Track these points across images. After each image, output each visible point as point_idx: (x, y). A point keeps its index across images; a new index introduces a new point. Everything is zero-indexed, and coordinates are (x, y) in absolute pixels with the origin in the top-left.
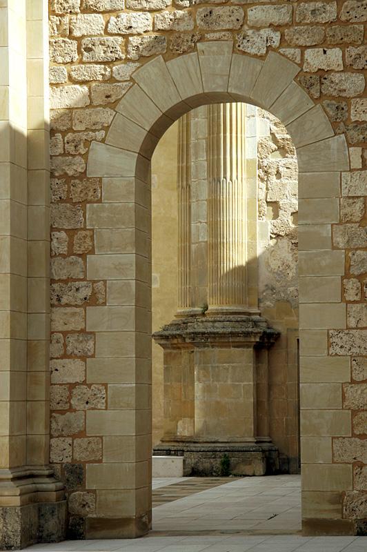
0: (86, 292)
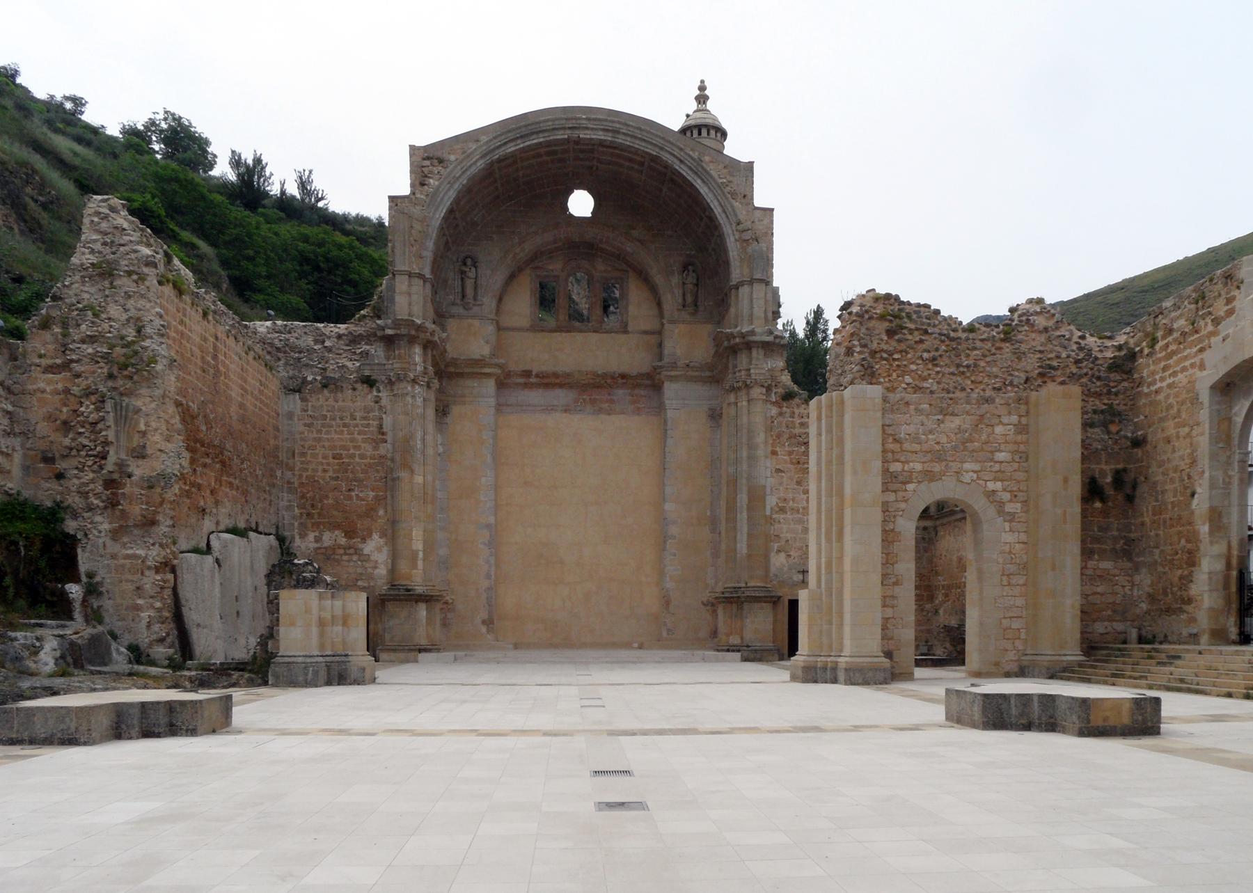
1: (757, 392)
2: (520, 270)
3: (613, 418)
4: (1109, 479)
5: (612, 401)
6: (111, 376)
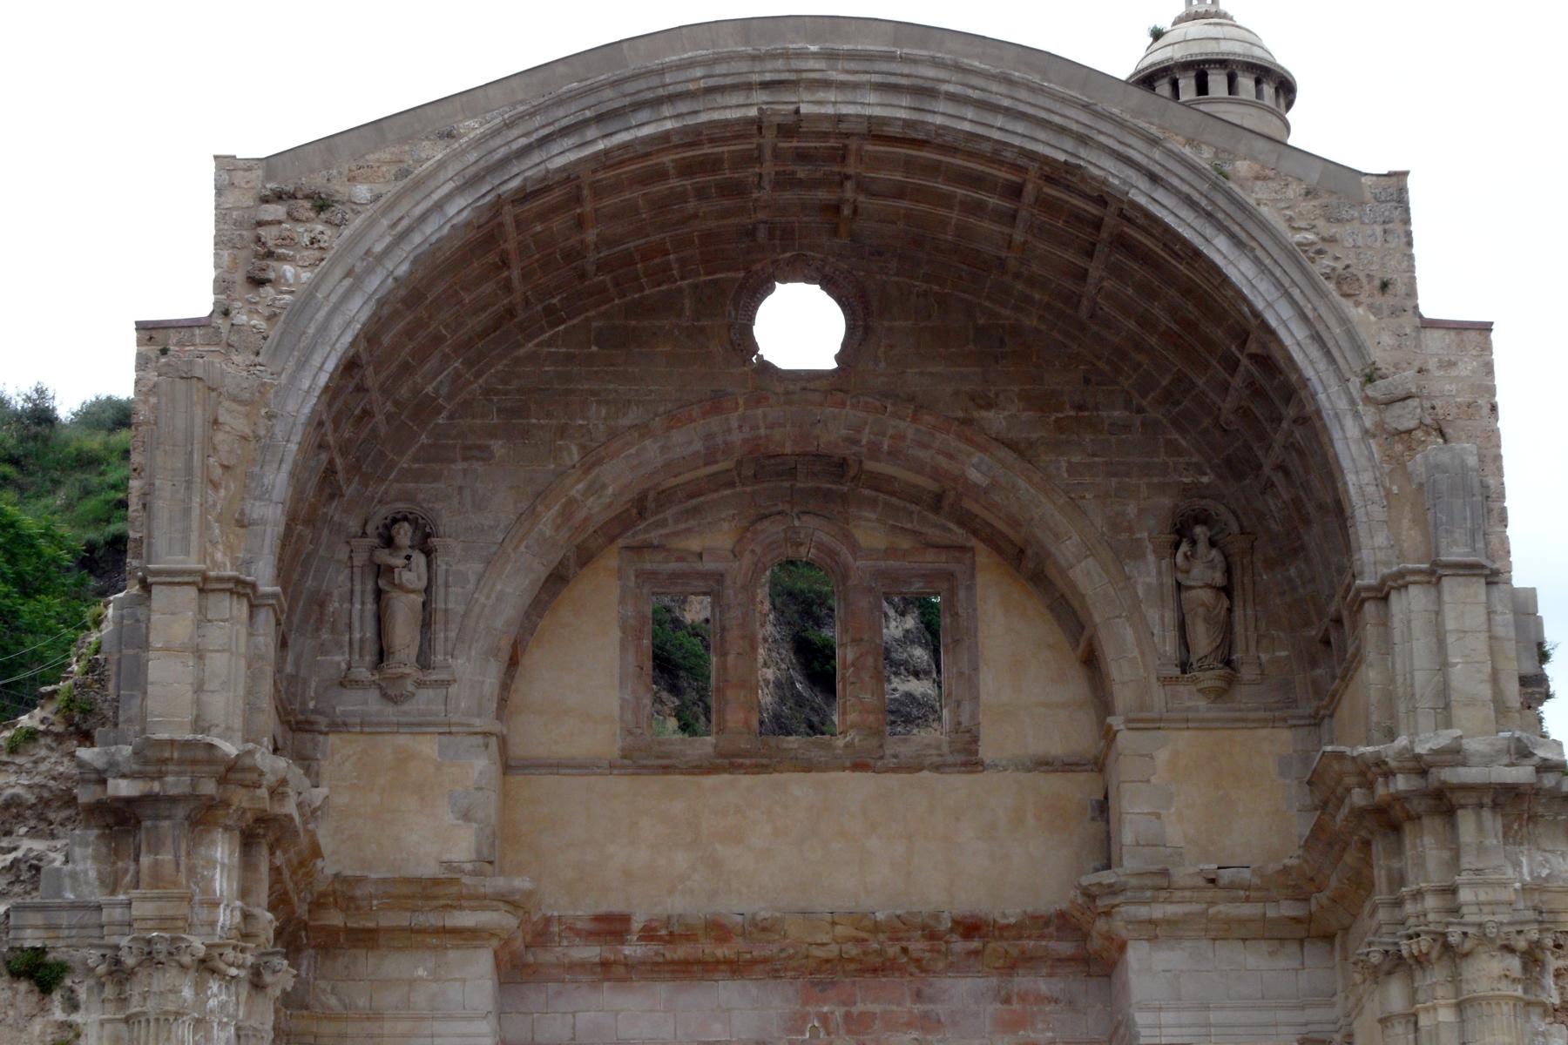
1: (1489, 972)
2: (585, 557)
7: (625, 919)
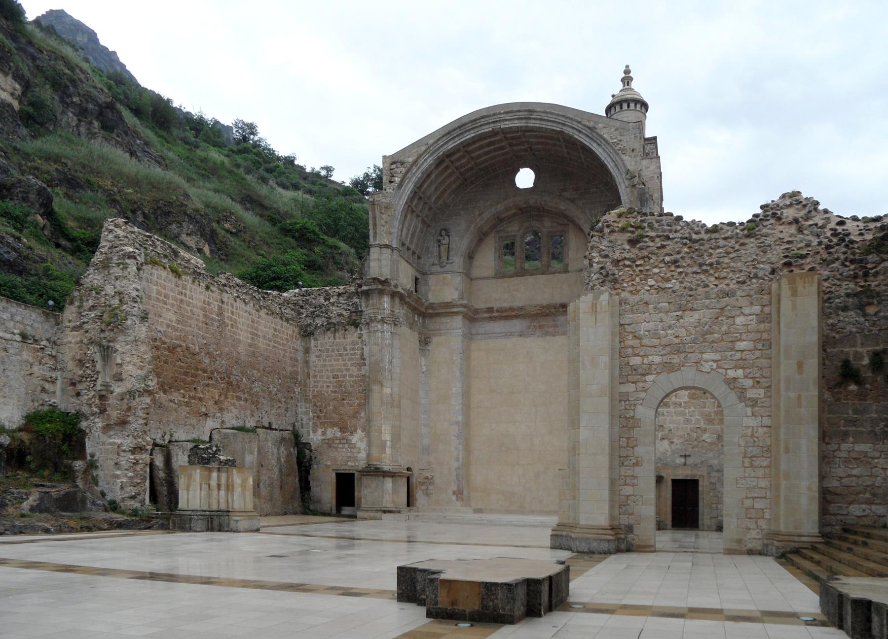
0: (634, 461)
3: (558, 338)
4: (866, 361)
5: (556, 326)
6: (102, 331)
7: (492, 308)
